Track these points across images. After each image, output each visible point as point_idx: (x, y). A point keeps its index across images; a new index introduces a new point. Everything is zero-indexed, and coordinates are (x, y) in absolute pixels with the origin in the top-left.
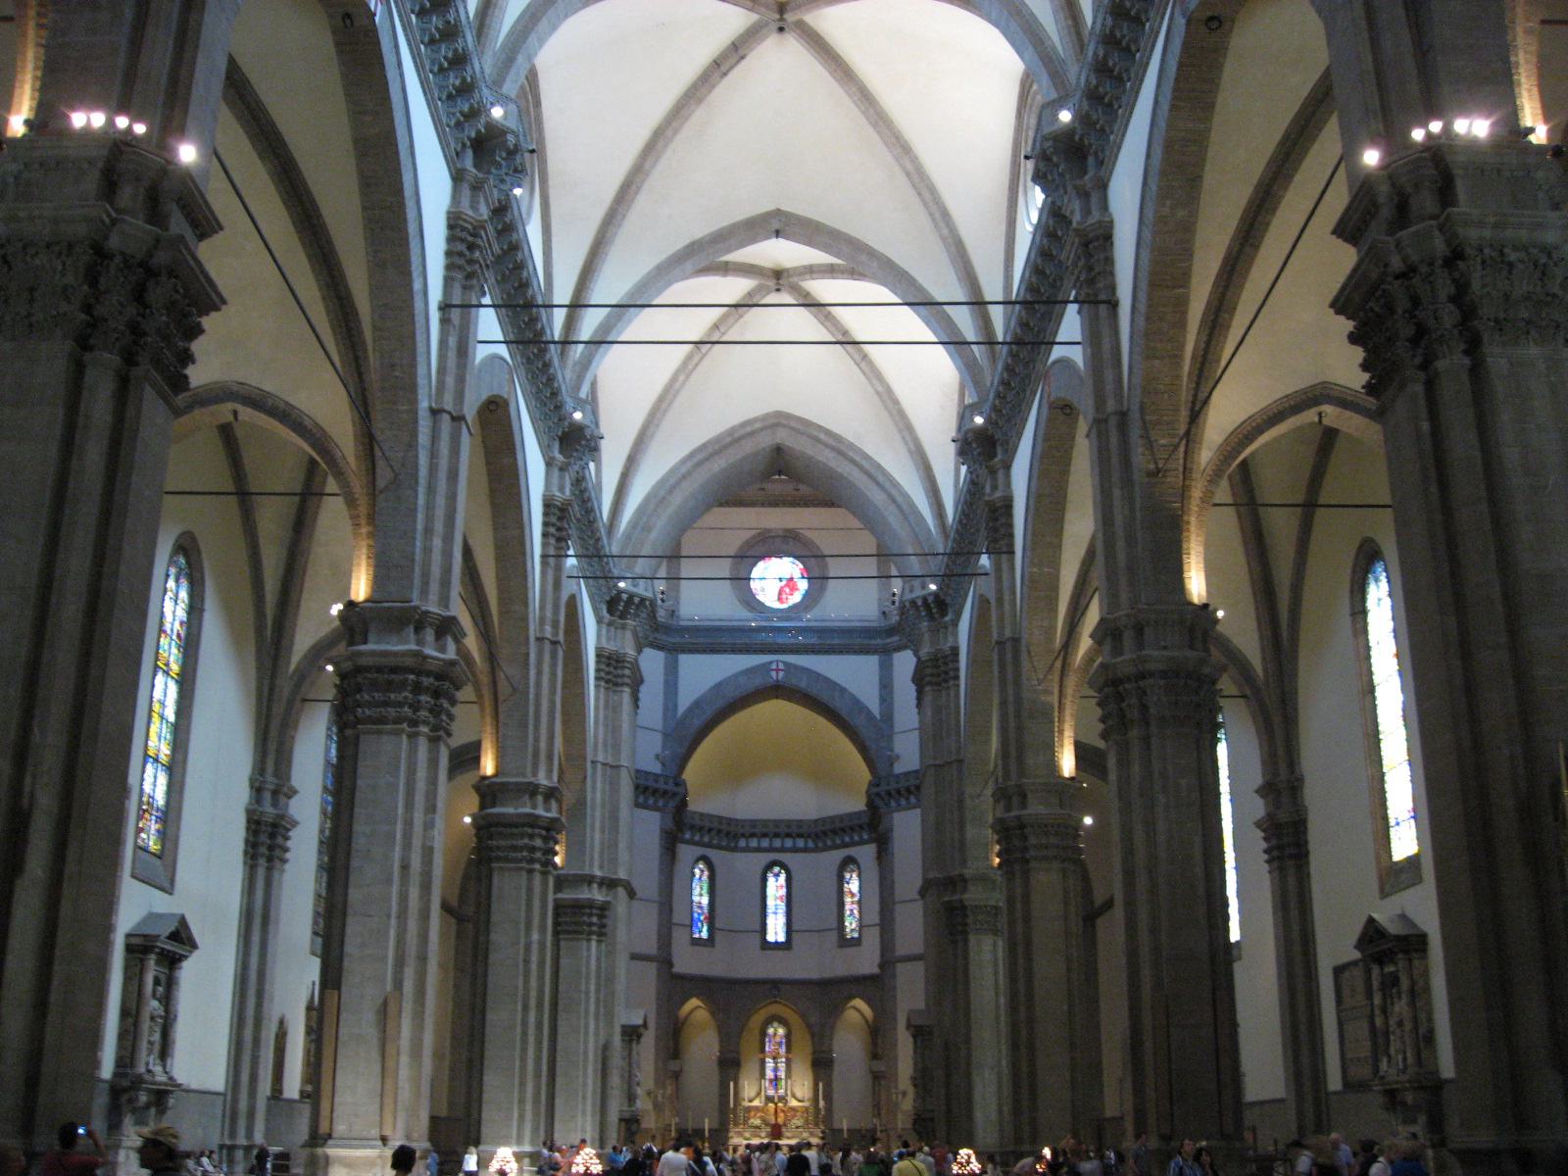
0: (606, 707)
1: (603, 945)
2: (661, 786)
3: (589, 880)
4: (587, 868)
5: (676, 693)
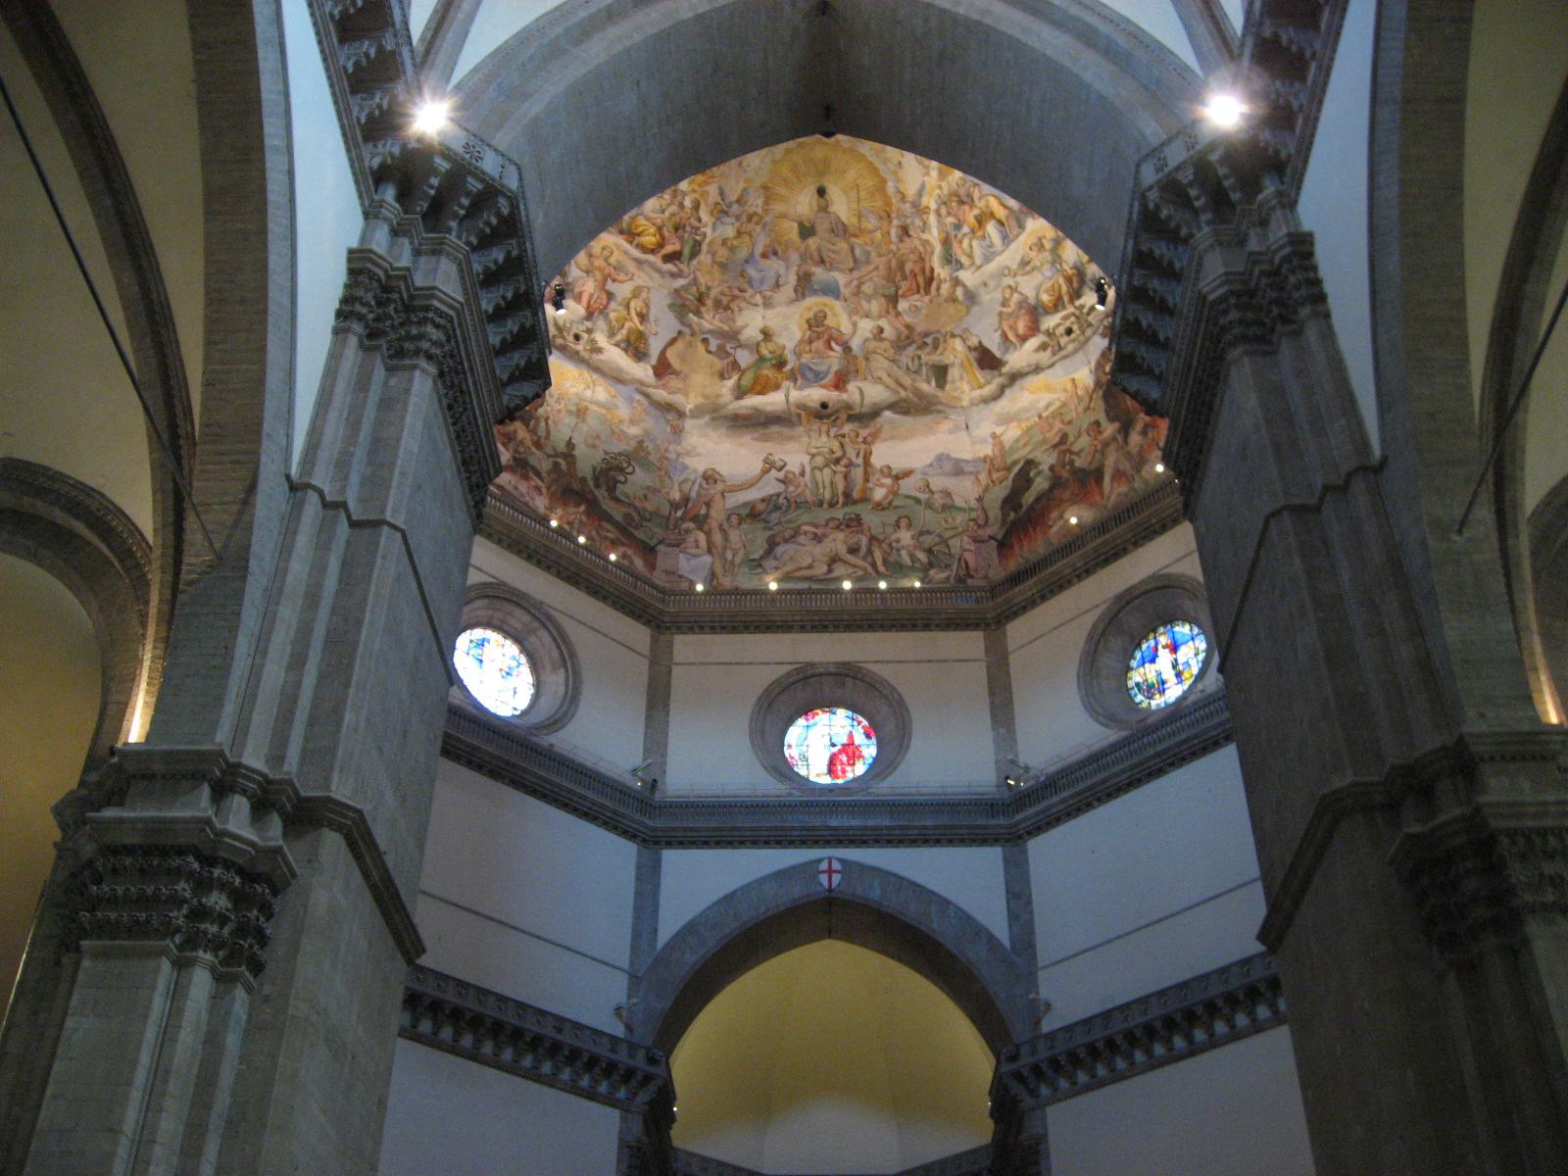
0: (362, 384)
1: (240, 993)
2: (622, 1057)
3: (225, 780)
4: (222, 736)
5: (656, 911)
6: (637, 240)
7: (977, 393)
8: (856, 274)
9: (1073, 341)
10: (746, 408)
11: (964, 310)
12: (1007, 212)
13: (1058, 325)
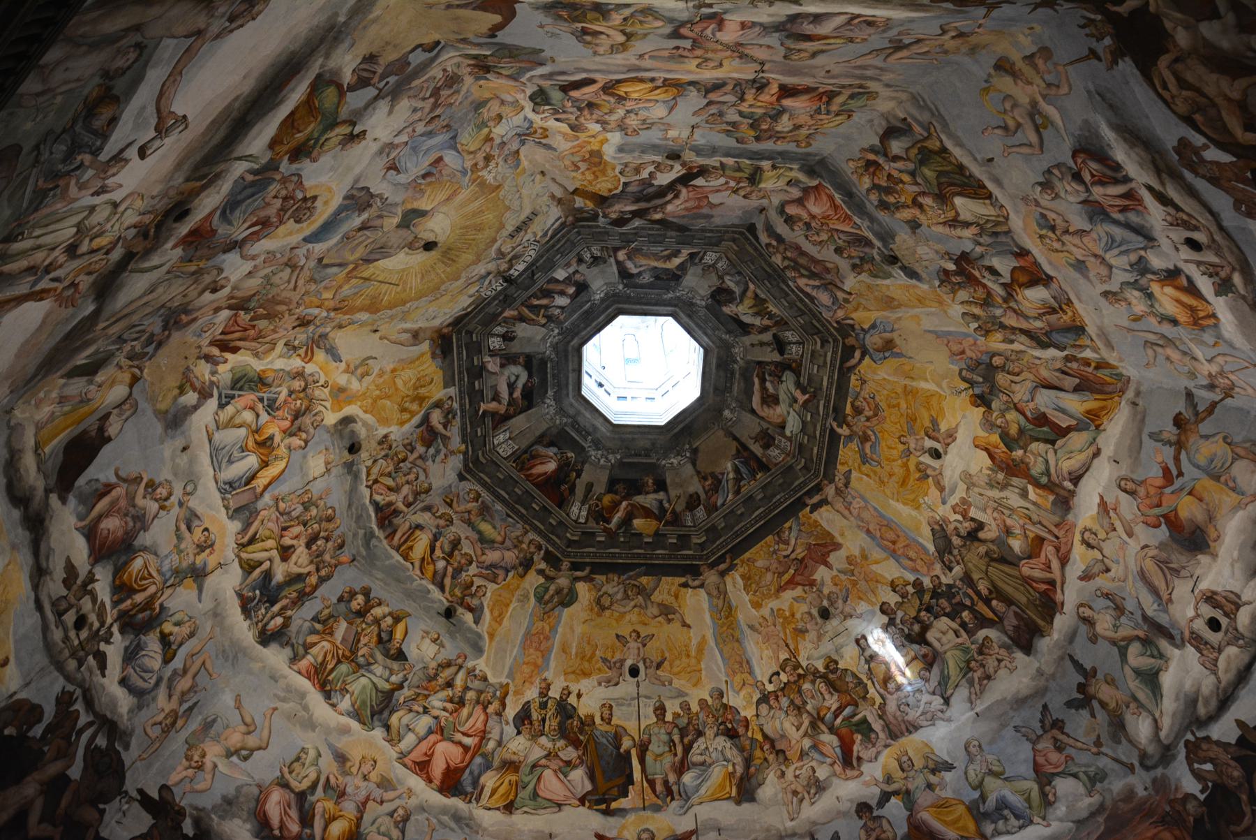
6: (659, 83)
7: (32, 443)
8: (312, 264)
9: (66, 638)
10: (293, 90)
11: (162, 406)
12: (259, 490)
13: (94, 600)
